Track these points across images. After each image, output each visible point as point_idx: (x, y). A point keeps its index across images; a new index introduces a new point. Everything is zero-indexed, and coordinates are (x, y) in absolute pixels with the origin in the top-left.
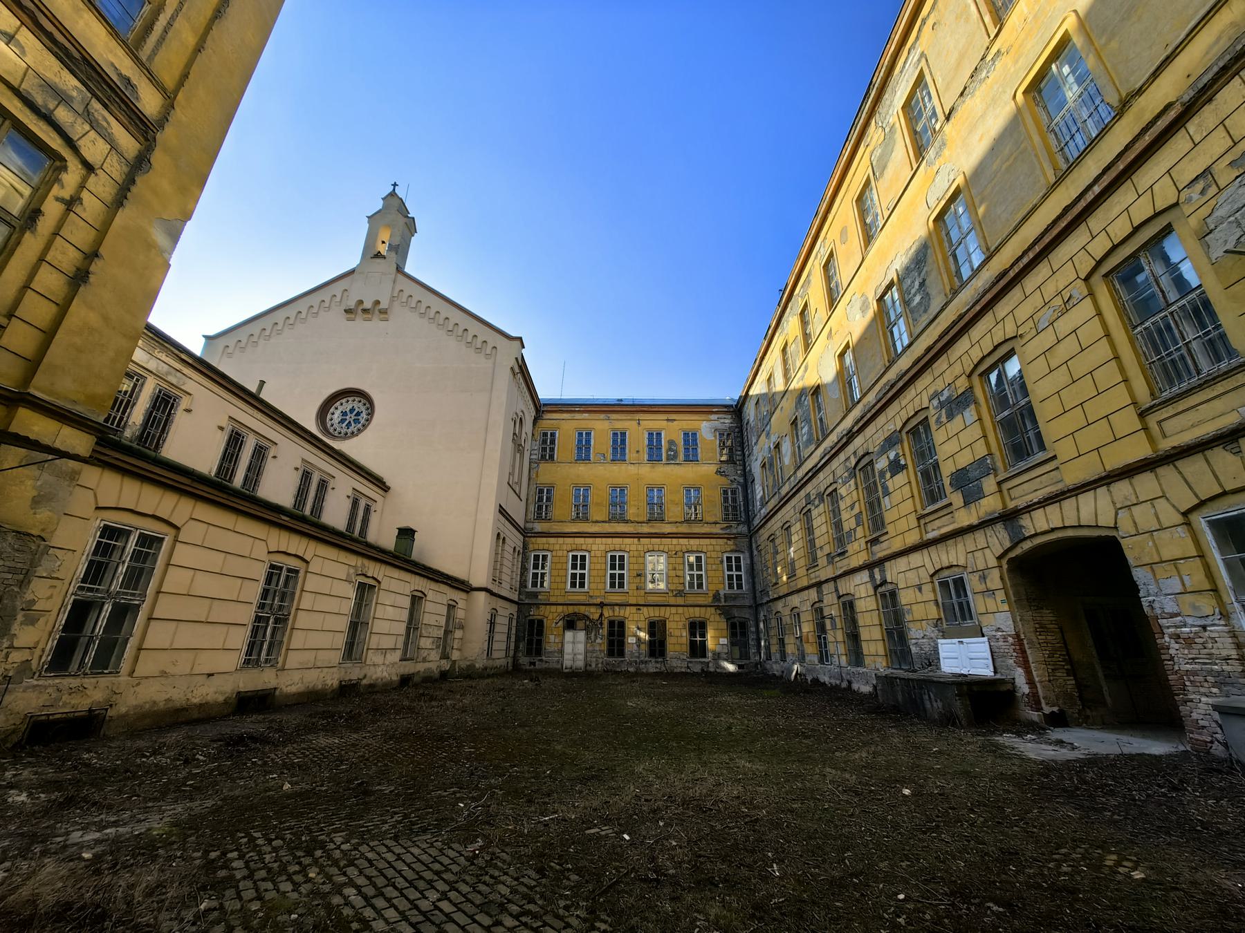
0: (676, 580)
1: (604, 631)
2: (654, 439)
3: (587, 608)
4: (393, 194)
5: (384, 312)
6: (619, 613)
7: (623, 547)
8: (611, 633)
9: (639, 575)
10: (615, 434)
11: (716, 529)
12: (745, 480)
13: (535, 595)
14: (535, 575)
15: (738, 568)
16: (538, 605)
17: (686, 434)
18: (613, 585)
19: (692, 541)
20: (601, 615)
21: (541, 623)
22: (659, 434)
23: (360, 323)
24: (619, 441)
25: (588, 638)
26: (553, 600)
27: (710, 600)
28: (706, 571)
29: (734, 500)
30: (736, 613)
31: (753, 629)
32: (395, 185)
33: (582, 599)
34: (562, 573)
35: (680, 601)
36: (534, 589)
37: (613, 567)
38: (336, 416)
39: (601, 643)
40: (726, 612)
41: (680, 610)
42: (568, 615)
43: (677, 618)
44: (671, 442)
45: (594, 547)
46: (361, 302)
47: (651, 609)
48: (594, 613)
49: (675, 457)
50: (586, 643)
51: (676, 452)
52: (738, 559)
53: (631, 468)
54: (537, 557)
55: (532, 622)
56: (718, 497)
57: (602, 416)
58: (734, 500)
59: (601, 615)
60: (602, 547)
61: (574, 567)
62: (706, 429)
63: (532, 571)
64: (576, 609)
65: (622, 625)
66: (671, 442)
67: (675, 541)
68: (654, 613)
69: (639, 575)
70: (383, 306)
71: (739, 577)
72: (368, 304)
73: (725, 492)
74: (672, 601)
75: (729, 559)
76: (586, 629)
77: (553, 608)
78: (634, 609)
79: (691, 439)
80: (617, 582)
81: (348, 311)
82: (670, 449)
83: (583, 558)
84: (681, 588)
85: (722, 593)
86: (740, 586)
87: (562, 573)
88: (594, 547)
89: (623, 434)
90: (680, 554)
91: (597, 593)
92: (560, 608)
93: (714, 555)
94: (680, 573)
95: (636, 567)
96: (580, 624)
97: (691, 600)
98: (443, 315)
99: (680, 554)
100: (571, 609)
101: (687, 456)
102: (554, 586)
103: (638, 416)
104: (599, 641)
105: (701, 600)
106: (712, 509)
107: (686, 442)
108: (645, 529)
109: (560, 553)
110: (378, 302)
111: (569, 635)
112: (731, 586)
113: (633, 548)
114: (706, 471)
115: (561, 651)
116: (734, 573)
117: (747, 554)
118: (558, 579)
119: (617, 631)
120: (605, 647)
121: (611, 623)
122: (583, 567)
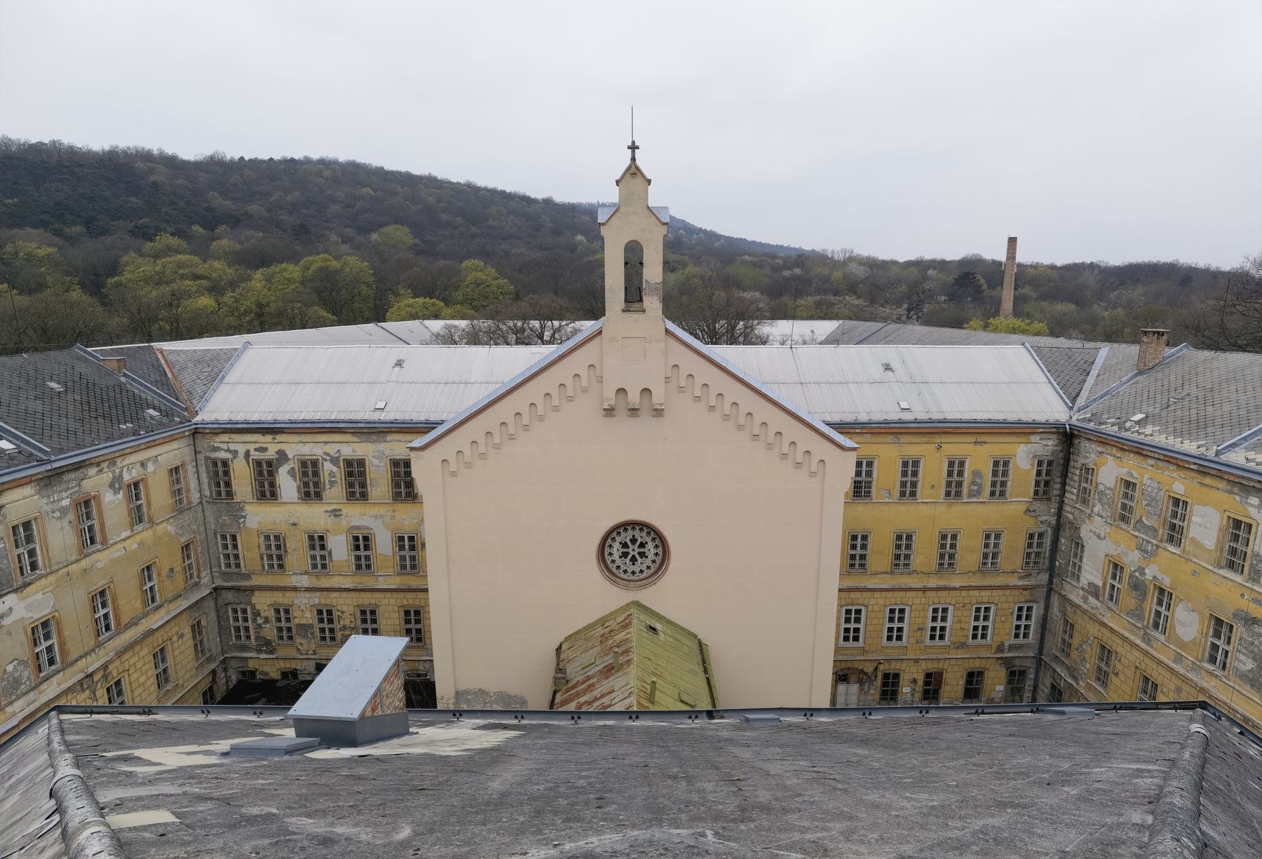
0: (960, 633)
2: (956, 467)
4: (633, 171)
5: (658, 412)
6: (893, 667)
7: (905, 601)
8: (885, 684)
10: (905, 464)
11: (1014, 581)
12: (1058, 520)
15: (1028, 617)
17: (996, 463)
19: (983, 593)
20: (876, 668)
22: (962, 464)
23: (621, 422)
24: (910, 468)
25: (861, 690)
28: (994, 622)
29: (1040, 545)
30: (1017, 662)
31: (1032, 676)
32: (633, 147)
37: (891, 620)
38: (614, 551)
39: (874, 691)
40: (1007, 662)
43: (955, 669)
44: (977, 474)
45: (873, 602)
46: (621, 391)
48: (869, 669)
49: (979, 493)
51: (980, 486)
52: (1029, 609)
53: (923, 508)
56: (1022, 541)
57: (890, 439)
58: (1040, 545)
59: (876, 668)
60: (881, 601)
62: (1024, 457)
65: (896, 676)
66: (977, 474)
67: (964, 593)
68: (932, 667)
70: (658, 397)
71: (1027, 627)
72: (634, 397)
73: (1031, 536)
75: (1020, 609)
76: (860, 682)
78: (912, 663)
79: (1001, 467)
80: (895, 634)
81: (610, 412)
82: (974, 483)
83: (858, 612)
85: (1007, 644)
86: (1026, 636)
88: (873, 602)
89: (916, 463)
90: (968, 606)
93: (1006, 606)
96: (853, 678)
98: (743, 410)
101: (992, 494)
103: (937, 439)
104: (872, 691)
106: (1012, 551)
107: (995, 473)
108: (933, 582)
110: (646, 391)
112: (1017, 636)
113: (917, 601)
114: (1015, 514)
117: (1042, 604)
120: (877, 697)
121: (886, 676)
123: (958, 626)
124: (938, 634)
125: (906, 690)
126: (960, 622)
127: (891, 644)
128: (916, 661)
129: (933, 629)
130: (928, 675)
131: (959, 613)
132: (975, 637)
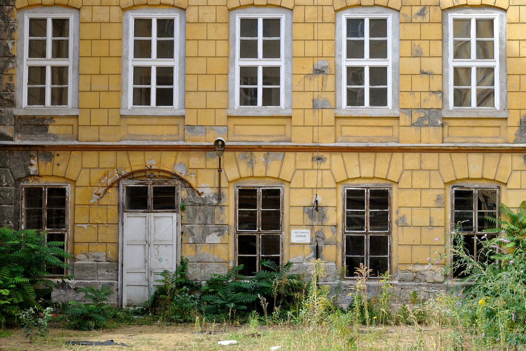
0: (421, 84)
1: (229, 214)
3: (181, 157)
6: (262, 172)
8: (246, 220)
9: (319, 71)
13: (40, 124)
14: (37, 74)
16: (46, 152)
18: (248, 97)
21: (58, 195)
26: (87, 137)
27: (512, 133)
28: (505, 58)
33: (165, 135)
34: (109, 66)
35: (430, 137)
36: (37, 110)
37: (248, 50)
41: (431, 160)
42: (131, 175)
47: (351, 158)
50: (182, 243)
54: (37, 26)
55: (34, 194)
61: (142, 50)
63: (26, 62)
64: (152, 160)
65: (273, 197)
68: (364, 172)
69: (319, 71)
74: (409, 137)
77: (90, 158)
78: (305, 160)
80: (260, 89)
84: (433, 102)
87: (109, 66)
91: (207, 119)
92: (108, 158)
94: (433, 65)
95: (312, 49)
97: (458, 137)
99: (435, 14)
100: (137, 161)
102: (91, 100)
105: (487, 137)
109: (101, 14)
111: (135, 223)
115: (115, 265)
116: (474, 63)
118: (100, 83)
119: (261, 208)
121: (246, 197)
122: (166, 50)
123: (413, 65)
124: (369, 88)
125: (296, 236)
126: (417, 54)
127: (250, 110)
128: (317, 151)
129: (355, 75)
130: (354, 199)
131: (412, 31)
132: (461, 98)
